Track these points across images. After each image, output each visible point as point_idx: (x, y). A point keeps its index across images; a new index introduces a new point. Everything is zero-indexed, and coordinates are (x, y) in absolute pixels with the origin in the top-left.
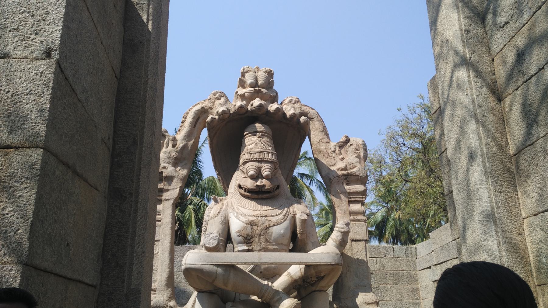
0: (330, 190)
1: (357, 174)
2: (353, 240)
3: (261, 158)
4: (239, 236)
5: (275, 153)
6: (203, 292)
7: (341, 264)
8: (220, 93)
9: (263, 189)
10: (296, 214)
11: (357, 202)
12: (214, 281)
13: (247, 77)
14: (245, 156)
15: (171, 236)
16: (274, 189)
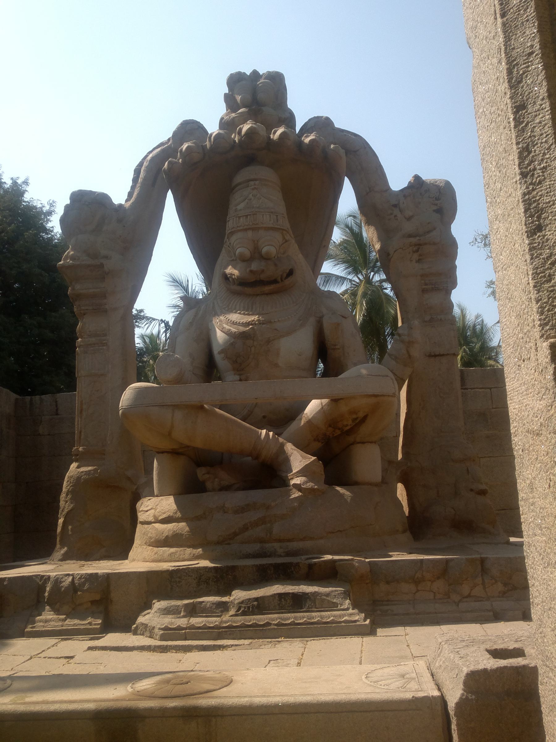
2: (430, 356)
3: (257, 224)
5: (283, 214)
6: (163, 452)
7: (394, 394)
9: (263, 277)
10: (323, 316)
12: (170, 434)
14: (230, 223)
16: (282, 276)
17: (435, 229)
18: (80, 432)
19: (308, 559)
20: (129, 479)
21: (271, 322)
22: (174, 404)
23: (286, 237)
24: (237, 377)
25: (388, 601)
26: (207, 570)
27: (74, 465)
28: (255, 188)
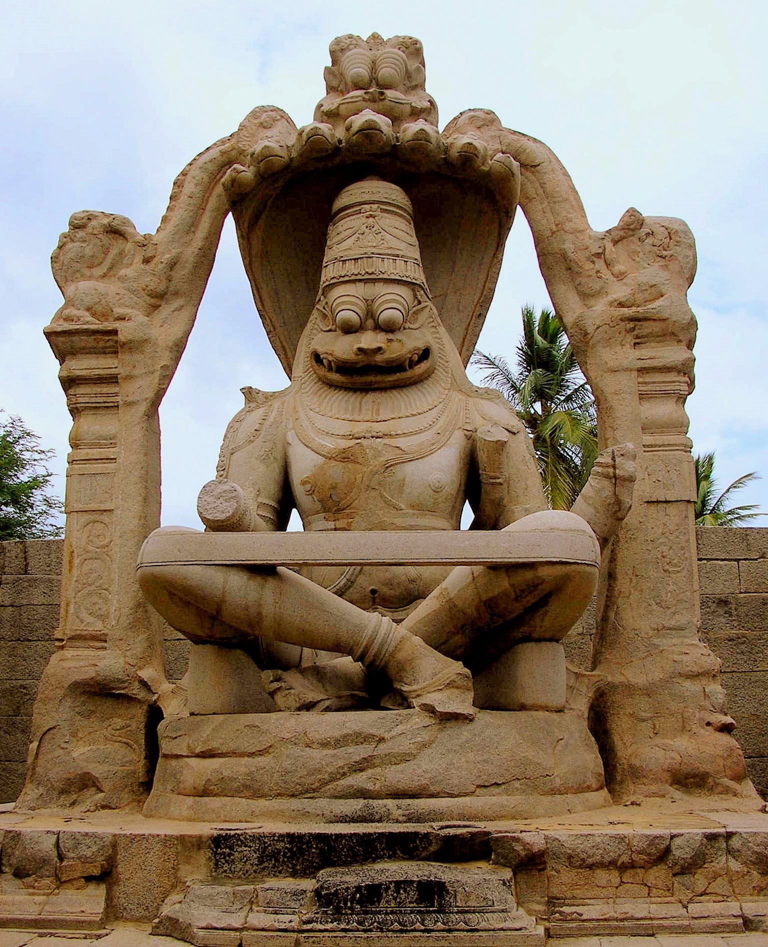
0: (586, 363)
1: (666, 315)
3: (373, 273)
4: (310, 493)
8: (272, 111)
9: (379, 358)
11: (666, 394)
12: (219, 611)
13: (346, 62)
14: (328, 269)
15: (140, 499)
16: (410, 359)
17: (662, 296)
18: (68, 605)
19: (442, 828)
20: (144, 684)
21: (390, 436)
22: (228, 563)
23: (419, 297)
24: (331, 525)
25: (574, 897)
26: (276, 838)
27: (54, 658)
28: (371, 216)
